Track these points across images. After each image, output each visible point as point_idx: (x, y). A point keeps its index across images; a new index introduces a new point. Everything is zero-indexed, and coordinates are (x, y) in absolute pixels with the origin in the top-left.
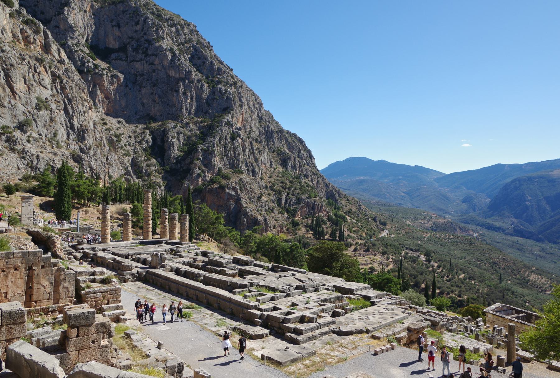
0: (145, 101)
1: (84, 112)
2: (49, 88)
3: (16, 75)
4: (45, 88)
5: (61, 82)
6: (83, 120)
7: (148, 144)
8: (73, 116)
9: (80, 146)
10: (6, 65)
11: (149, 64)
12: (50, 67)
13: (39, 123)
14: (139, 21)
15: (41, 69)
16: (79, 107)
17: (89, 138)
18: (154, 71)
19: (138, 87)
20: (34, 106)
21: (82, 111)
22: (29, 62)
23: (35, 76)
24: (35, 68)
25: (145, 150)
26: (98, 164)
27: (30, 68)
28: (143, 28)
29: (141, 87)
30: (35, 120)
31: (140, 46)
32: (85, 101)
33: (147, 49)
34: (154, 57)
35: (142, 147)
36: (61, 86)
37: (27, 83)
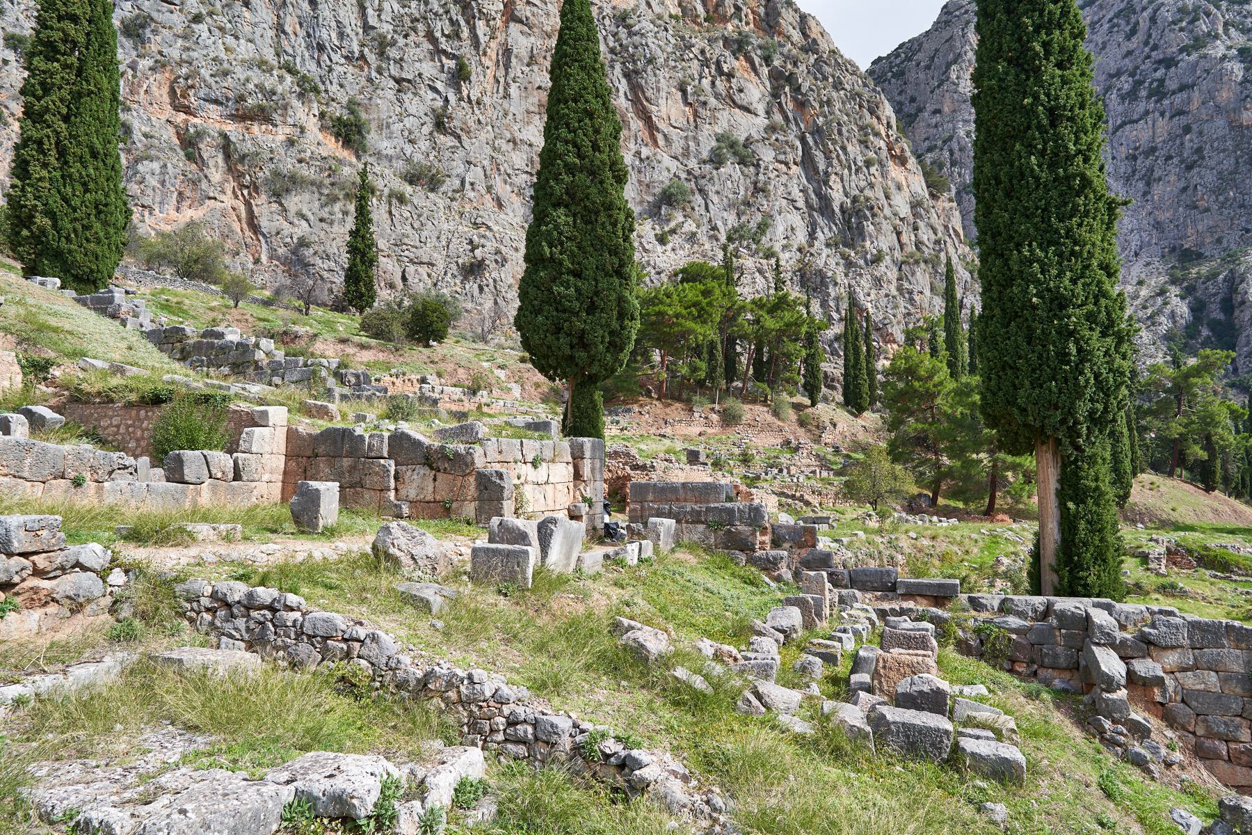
0: (1164, 216)
1: (868, 164)
2: (761, 112)
3: (658, 82)
4: (747, 110)
5: (797, 89)
6: (863, 184)
7: (1174, 322)
8: (827, 174)
9: (844, 257)
10: (634, 62)
11: (1171, 118)
12: (767, 60)
13: (715, 199)
14: (1137, 23)
15: (730, 63)
16: (850, 148)
17: (879, 230)
18: (1187, 129)
19: (1141, 185)
20: (705, 155)
21: (859, 158)
22: (703, 52)
23: (718, 83)
24: (718, 63)
25: (1169, 337)
26: (883, 292)
27: (705, 63)
28: (1150, 36)
29: (1148, 184)
30: (700, 191)
31: (1141, 83)
32: (877, 134)
33: (1161, 82)
34: (1184, 95)
35: (1155, 333)
36: (795, 99)
37: (690, 100)
